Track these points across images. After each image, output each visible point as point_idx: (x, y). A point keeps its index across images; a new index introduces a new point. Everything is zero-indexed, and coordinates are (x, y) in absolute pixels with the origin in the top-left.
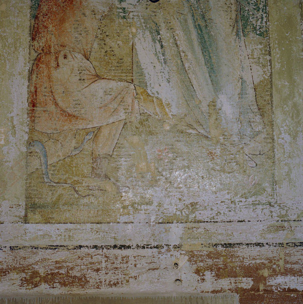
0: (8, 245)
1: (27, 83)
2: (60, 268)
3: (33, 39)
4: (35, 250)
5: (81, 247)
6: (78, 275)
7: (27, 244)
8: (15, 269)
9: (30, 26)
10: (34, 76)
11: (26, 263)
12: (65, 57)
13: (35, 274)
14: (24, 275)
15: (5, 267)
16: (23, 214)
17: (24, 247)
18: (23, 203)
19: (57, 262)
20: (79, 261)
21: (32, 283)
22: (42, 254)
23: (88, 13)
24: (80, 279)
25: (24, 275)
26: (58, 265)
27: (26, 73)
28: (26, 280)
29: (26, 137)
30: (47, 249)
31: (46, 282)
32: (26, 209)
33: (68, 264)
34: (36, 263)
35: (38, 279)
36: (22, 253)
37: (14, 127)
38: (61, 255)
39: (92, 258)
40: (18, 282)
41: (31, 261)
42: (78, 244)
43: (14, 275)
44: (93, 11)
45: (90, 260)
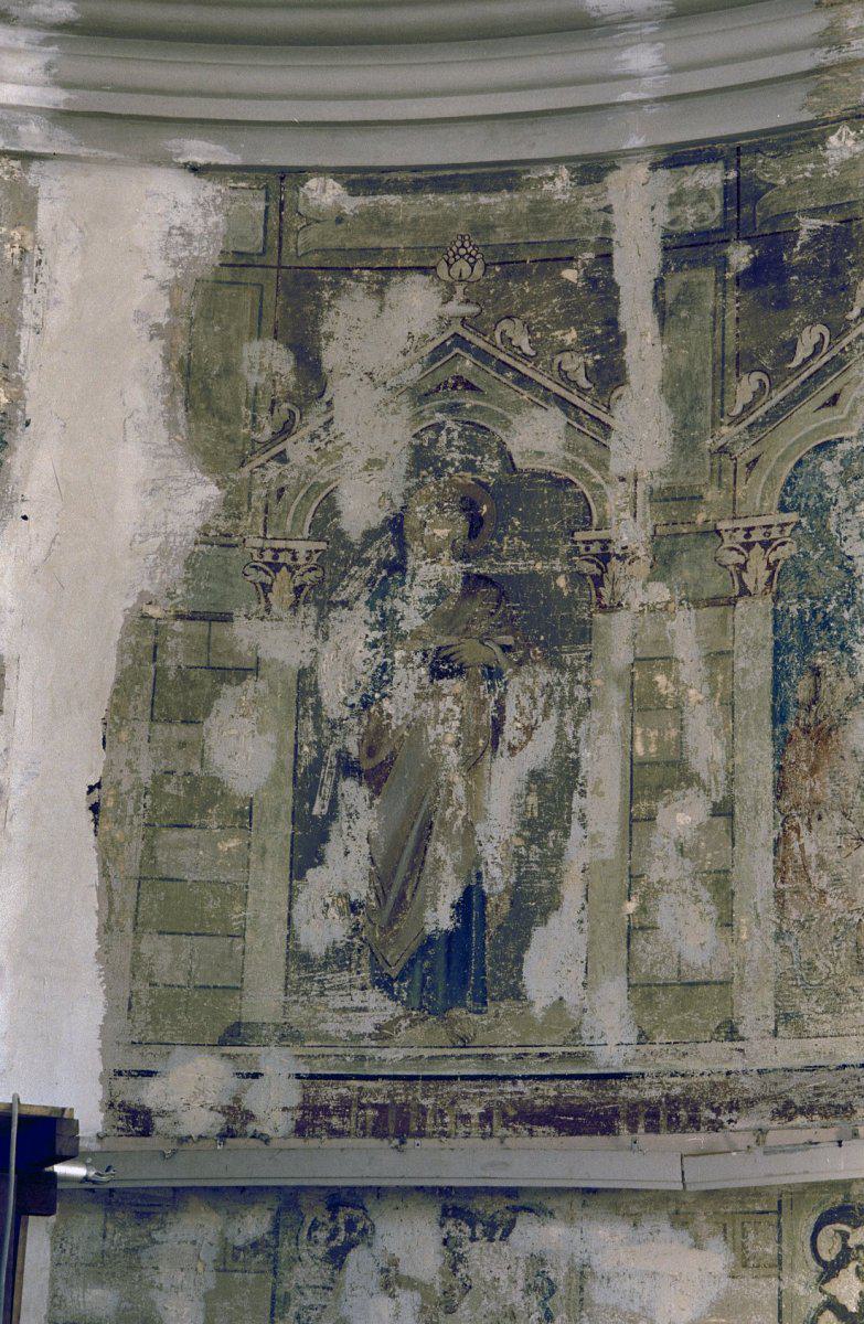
0: (755, 1069)
1: (772, 857)
2: (819, 1095)
3: (778, 798)
4: (788, 1074)
5: (845, 1066)
6: (842, 1103)
7: (778, 1066)
8: (764, 1098)
9: (774, 782)
10: (781, 848)
11: (776, 1090)
12: (820, 818)
13: (789, 1104)
14: (775, 1106)
15: (751, 1096)
16: (772, 1027)
17: (775, 1070)
18: (771, 1012)
19: (816, 1088)
20: (843, 1086)
21: (786, 1116)
22: (797, 1078)
23: (847, 755)
24: (845, 1109)
25: (775, 1106)
26: (817, 1092)
27: (771, 843)
28: (778, 1112)
29: (774, 929)
30: (802, 1070)
31: (803, 1113)
32: (776, 1021)
33: (829, 1090)
34: (790, 1090)
35: (792, 1110)
36: (772, 1077)
37: (758, 915)
38: (823, 1079)
39: (859, 1080)
40: (769, 1115)
41: (784, 1087)
42: (843, 1062)
43: (762, 1106)
44: (854, 752)
45: (857, 1083)
